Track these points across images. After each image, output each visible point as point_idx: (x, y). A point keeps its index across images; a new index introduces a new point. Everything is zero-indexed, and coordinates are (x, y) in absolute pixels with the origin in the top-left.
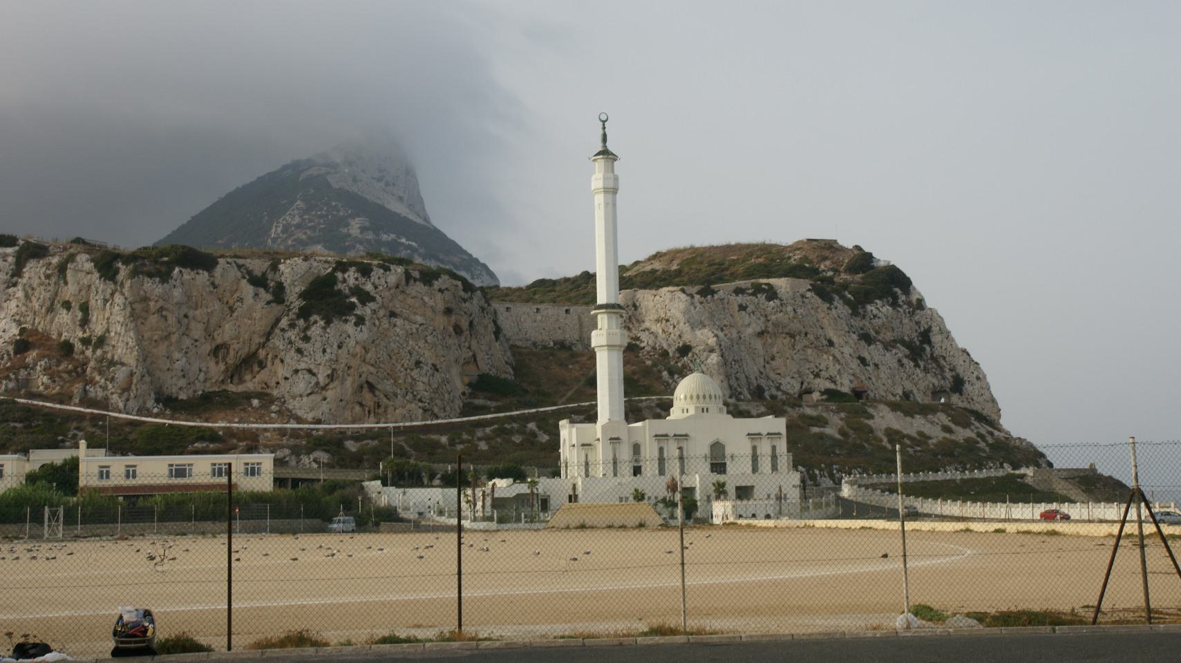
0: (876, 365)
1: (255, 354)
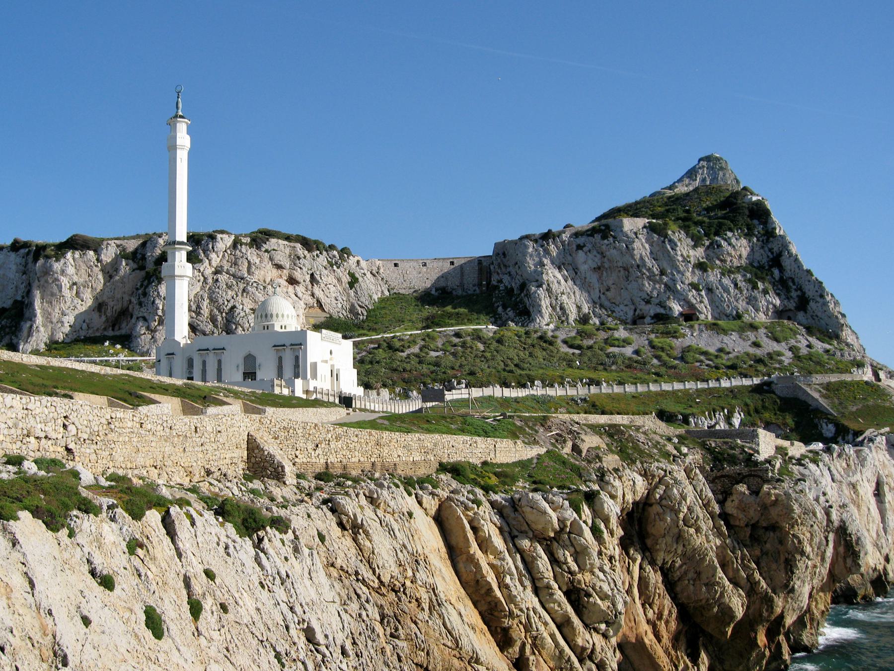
0: (710, 290)
1: (128, 308)
